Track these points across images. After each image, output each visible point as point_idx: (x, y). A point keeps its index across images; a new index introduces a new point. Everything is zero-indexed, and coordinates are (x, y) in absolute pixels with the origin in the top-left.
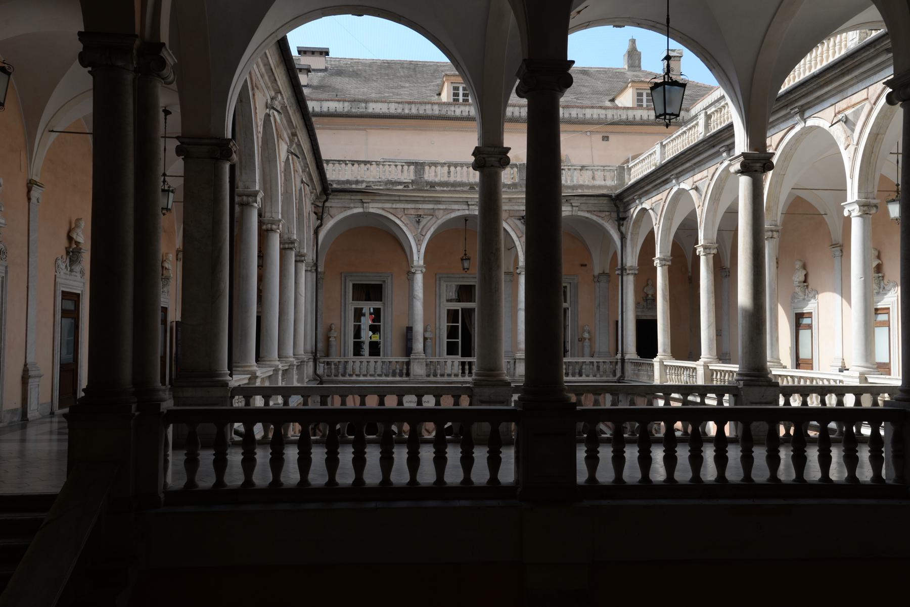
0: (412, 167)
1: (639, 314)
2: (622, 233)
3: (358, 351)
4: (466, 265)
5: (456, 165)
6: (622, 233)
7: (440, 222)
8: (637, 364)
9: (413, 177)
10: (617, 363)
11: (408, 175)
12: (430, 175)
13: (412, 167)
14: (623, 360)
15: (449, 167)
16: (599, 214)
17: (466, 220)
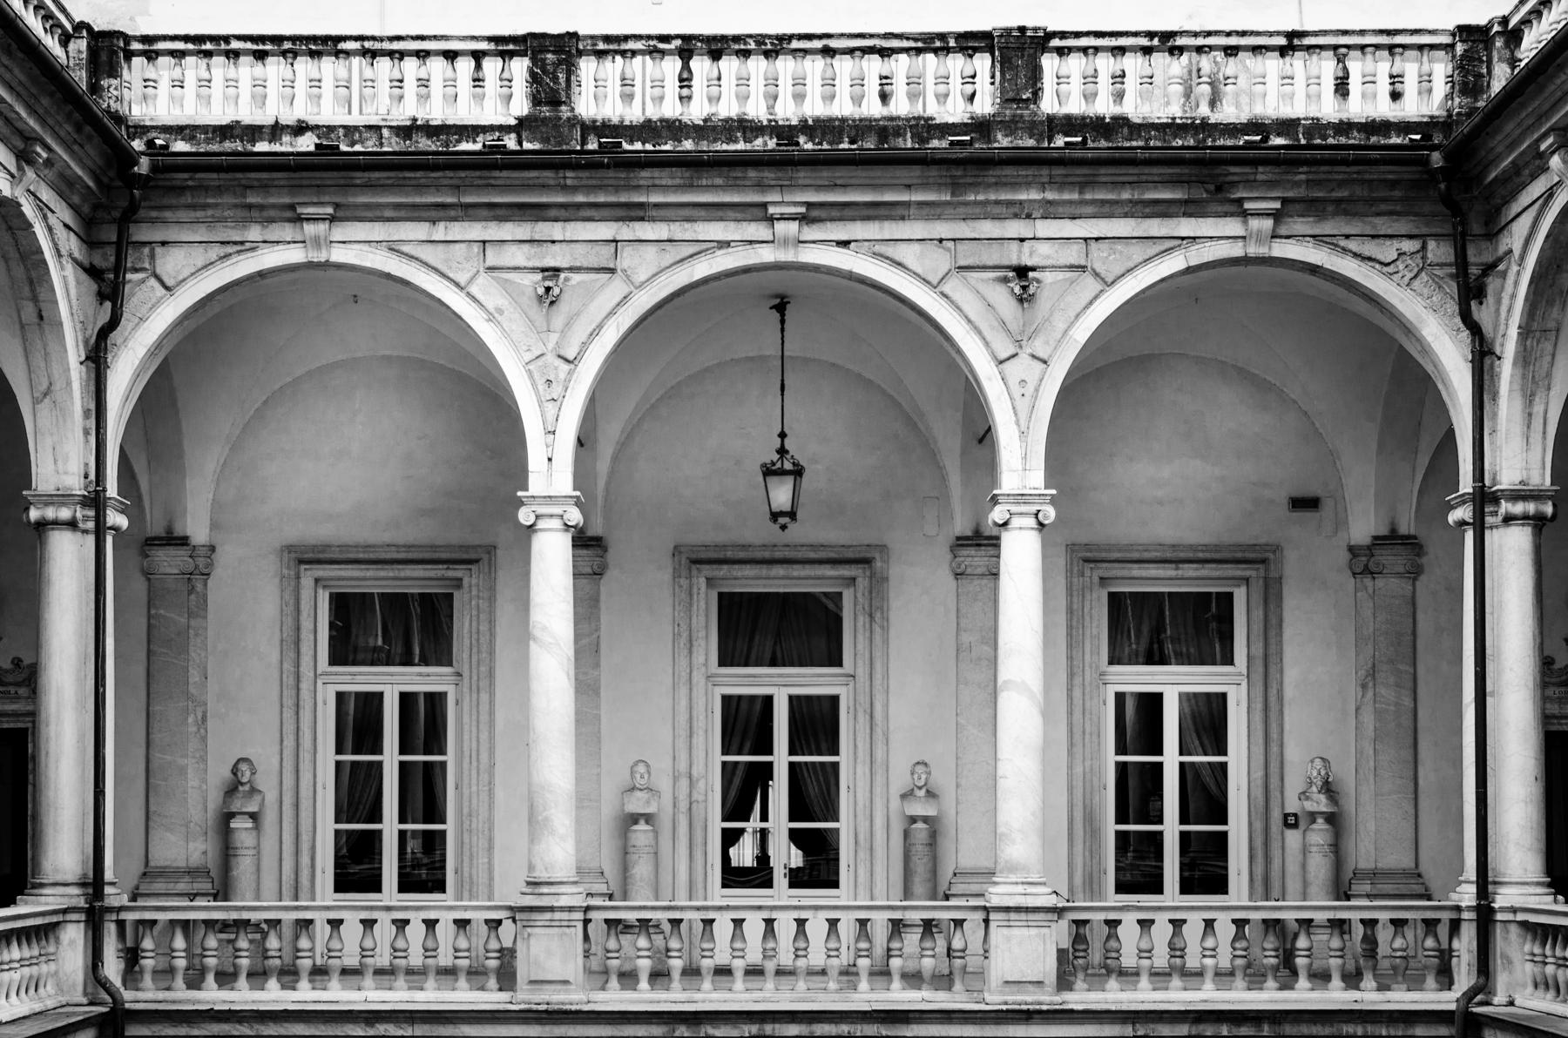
0: (520, 67)
1: (1554, 709)
2: (1474, 329)
3: (356, 868)
4: (781, 494)
5: (717, 47)
6: (1474, 329)
7: (645, 300)
8: (1543, 933)
9: (521, 106)
10: (1455, 926)
11: (498, 100)
12: (599, 94)
13: (520, 67)
14: (1485, 914)
15: (686, 54)
16: (1369, 248)
17: (781, 308)
